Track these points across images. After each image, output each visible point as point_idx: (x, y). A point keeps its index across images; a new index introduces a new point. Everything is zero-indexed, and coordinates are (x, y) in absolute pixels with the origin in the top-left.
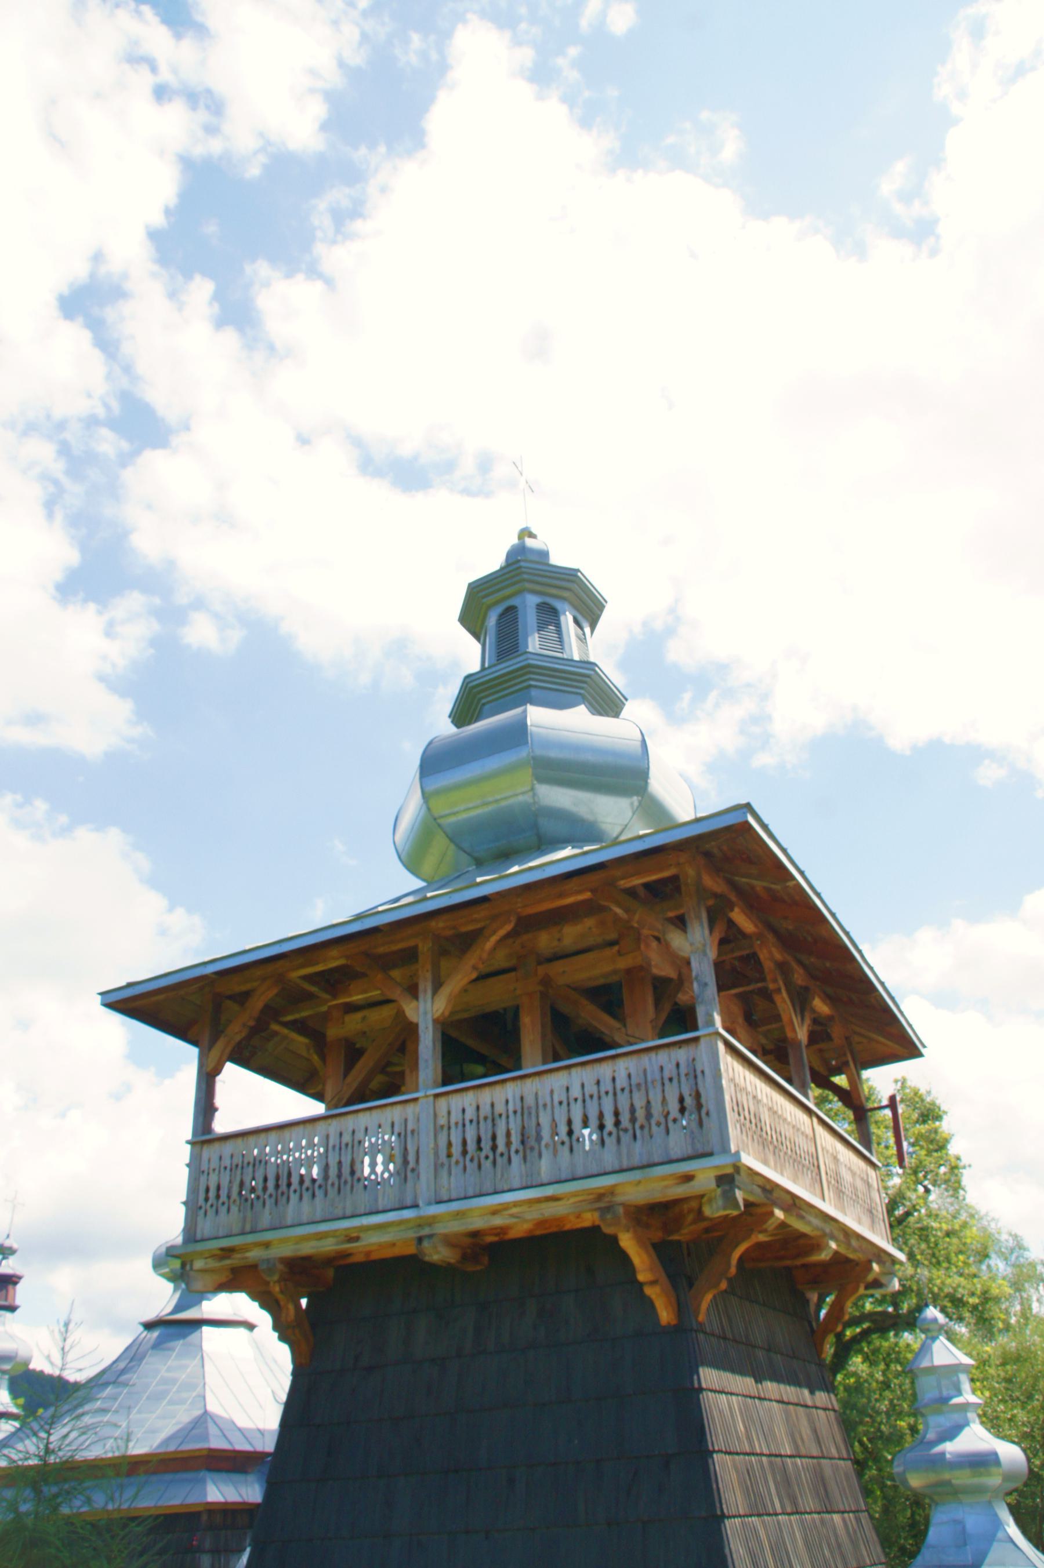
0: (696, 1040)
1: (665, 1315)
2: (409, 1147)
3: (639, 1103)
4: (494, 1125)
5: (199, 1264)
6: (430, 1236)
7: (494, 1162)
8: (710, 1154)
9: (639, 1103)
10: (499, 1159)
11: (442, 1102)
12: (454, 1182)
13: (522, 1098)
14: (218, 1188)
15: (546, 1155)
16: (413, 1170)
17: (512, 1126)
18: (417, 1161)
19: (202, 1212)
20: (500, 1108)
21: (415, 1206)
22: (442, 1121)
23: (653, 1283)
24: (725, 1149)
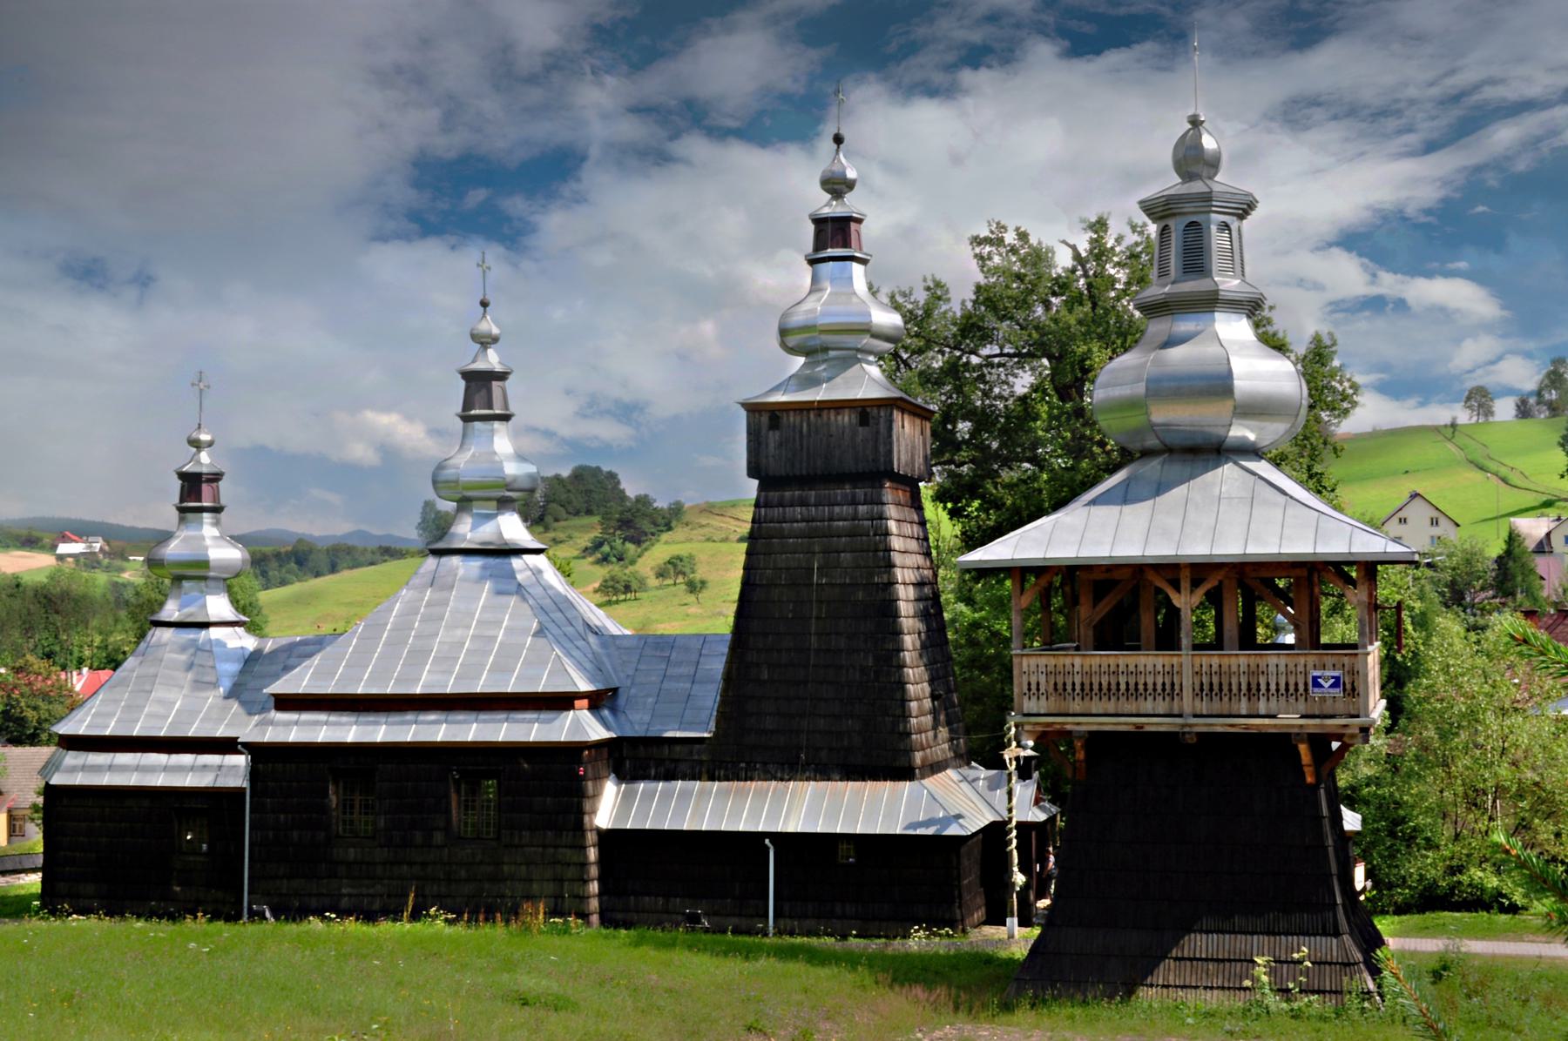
0: (1356, 654)
1: (1309, 779)
2: (1175, 681)
4: (1230, 677)
5: (1027, 728)
6: (1189, 733)
7: (1230, 699)
8: (1358, 716)
10: (1233, 698)
11: (1197, 661)
12: (1203, 707)
13: (1249, 666)
14: (1038, 684)
15: (1263, 700)
16: (1178, 694)
17: (1242, 680)
18: (1181, 690)
20: (1234, 669)
21: (1180, 716)
22: (1197, 669)
23: (1310, 766)
24: (1367, 716)
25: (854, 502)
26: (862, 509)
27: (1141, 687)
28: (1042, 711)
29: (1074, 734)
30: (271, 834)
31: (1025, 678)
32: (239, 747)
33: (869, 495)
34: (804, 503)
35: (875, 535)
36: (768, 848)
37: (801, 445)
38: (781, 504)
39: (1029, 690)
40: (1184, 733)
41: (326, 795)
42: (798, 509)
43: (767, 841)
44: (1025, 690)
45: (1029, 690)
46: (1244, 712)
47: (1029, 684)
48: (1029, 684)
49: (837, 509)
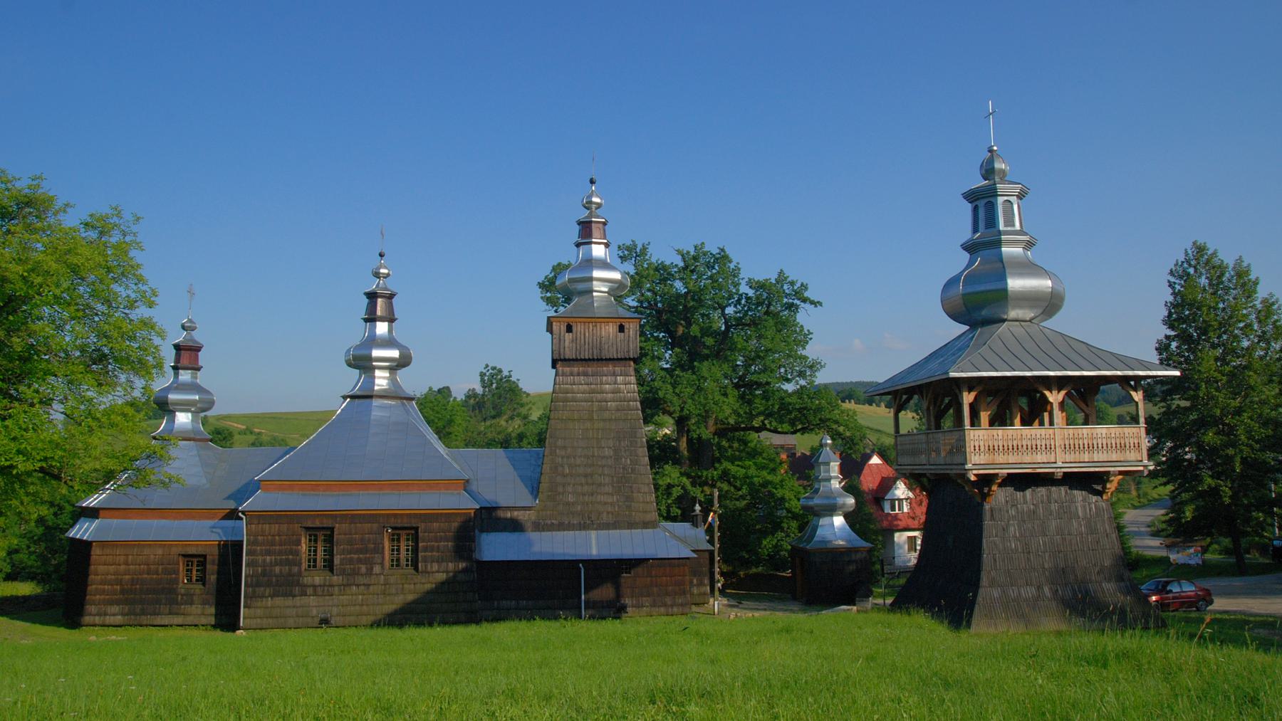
3: (1123, 442)
9: (1123, 442)
18: (1055, 448)
19: (973, 454)
25: (614, 375)
26: (620, 379)
27: (1034, 447)
28: (982, 463)
29: (1000, 475)
30: (260, 569)
31: (972, 442)
32: (240, 514)
33: (623, 372)
34: (586, 374)
35: (628, 393)
36: (580, 569)
37: (585, 342)
38: (572, 374)
39: (975, 450)
40: (1057, 473)
41: (299, 543)
42: (582, 378)
43: (581, 565)
44: (972, 450)
45: (975, 450)
46: (1086, 460)
47: (975, 446)
48: (975, 446)
49: (604, 378)
